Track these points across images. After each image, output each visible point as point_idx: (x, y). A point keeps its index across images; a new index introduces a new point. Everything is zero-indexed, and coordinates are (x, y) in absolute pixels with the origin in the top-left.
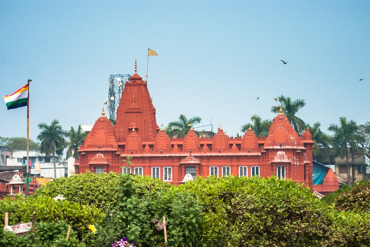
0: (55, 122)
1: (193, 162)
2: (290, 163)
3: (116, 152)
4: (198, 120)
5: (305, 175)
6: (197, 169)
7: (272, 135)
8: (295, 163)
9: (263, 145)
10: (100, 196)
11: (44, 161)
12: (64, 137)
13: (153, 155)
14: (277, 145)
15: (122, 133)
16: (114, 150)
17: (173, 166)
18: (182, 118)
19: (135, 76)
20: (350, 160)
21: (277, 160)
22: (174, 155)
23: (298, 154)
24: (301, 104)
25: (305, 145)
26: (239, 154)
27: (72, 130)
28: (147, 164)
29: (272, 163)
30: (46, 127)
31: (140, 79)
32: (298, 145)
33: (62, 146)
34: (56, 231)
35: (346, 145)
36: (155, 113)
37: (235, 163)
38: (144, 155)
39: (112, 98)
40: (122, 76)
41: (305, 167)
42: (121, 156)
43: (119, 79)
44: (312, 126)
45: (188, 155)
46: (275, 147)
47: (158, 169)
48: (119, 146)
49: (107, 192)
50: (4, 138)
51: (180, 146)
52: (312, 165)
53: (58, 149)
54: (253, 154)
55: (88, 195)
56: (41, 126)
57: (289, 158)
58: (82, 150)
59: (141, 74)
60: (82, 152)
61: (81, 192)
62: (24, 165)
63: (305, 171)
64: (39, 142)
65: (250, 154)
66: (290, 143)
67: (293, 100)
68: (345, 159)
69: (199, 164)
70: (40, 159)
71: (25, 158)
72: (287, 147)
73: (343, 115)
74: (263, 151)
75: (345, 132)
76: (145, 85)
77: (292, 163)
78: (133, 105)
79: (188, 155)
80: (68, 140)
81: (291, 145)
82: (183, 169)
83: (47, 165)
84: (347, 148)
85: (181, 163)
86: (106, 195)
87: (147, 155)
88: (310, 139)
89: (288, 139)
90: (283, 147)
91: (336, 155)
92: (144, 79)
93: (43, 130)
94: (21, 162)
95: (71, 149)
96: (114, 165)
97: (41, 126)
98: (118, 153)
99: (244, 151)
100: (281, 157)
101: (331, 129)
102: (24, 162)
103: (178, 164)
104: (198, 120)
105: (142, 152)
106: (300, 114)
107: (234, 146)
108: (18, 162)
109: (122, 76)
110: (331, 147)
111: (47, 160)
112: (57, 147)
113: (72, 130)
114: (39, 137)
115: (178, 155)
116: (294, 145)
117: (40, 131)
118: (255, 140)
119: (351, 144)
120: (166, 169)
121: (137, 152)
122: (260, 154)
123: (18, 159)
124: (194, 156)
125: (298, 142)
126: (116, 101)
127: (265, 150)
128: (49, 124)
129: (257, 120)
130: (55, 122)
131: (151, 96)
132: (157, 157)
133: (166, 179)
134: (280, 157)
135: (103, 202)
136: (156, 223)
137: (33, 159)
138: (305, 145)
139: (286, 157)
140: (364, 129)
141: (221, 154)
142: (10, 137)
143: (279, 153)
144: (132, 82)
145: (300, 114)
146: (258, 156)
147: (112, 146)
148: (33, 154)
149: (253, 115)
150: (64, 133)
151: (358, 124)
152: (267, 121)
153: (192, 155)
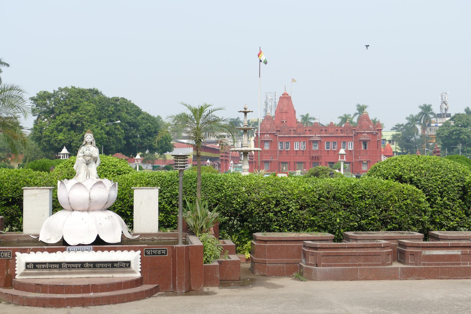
28: (292, 141)
31: (288, 95)
32: (374, 130)
38: (291, 135)
59: (288, 92)
76: (290, 98)
81: (371, 130)
92: (289, 95)
121: (287, 134)
125: (374, 128)
131: (293, 104)
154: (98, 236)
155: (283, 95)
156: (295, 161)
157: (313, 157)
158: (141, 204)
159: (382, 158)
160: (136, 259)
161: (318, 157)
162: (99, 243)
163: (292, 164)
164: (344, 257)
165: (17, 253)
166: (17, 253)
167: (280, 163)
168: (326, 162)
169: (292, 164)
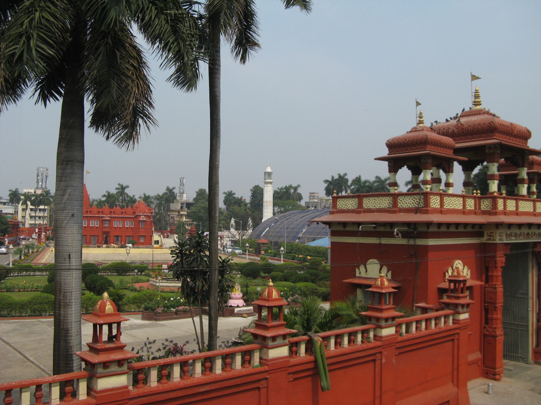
0: (17, 189)
24: (128, 187)
30: (12, 191)
44: (132, 196)
56: (10, 191)
67: (124, 185)
80: (22, 197)
83: (5, 206)
93: (11, 192)
97: (10, 191)
100: (143, 218)
106: (127, 191)
109: (43, 168)
117: (9, 193)
128: (14, 190)
129: (109, 193)
130: (17, 189)
134: (142, 218)
145: (127, 191)
169: (88, 237)
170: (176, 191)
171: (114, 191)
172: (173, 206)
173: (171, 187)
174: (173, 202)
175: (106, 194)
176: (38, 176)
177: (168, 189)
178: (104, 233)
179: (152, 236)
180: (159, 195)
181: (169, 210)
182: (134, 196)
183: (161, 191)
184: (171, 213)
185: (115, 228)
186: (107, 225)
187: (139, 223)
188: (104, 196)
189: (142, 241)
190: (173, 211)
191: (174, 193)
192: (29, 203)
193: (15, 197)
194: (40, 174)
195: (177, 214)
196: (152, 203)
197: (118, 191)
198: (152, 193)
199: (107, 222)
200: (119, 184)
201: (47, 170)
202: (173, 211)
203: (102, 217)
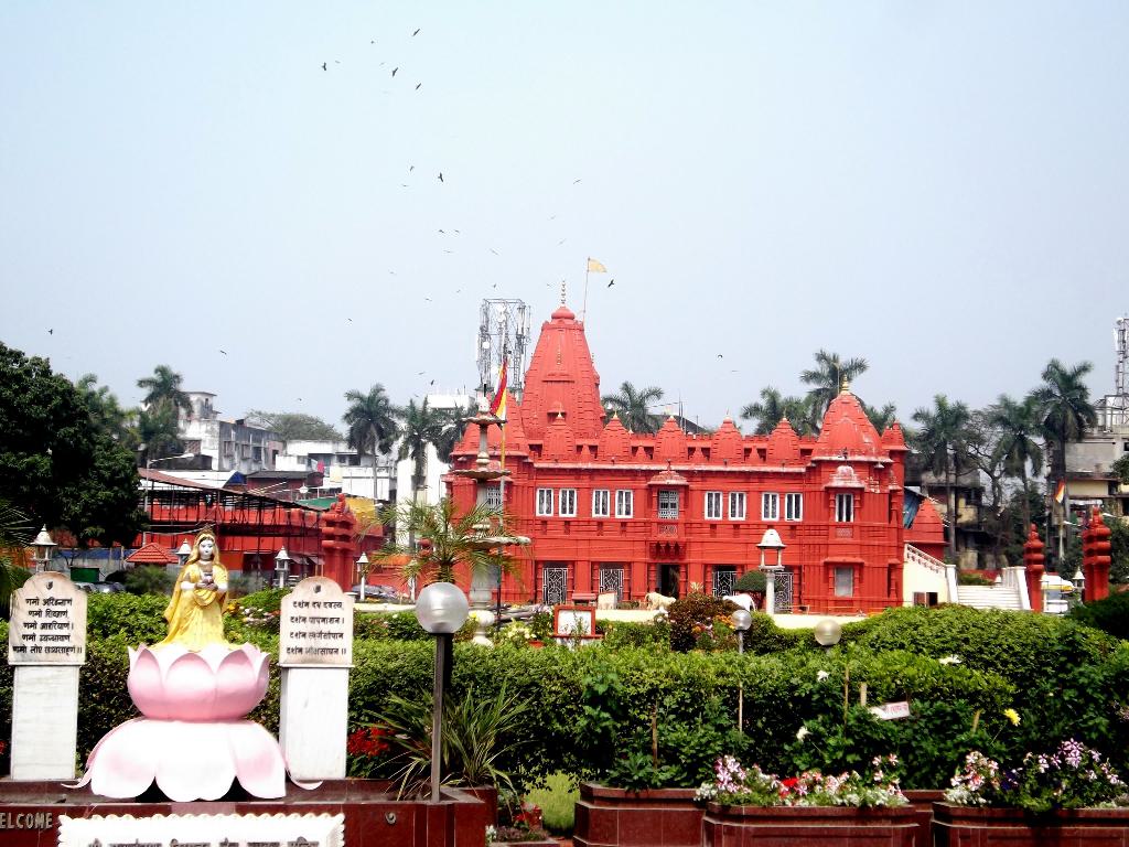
0: (378, 390)
1: (673, 482)
2: (861, 489)
3: (526, 457)
4: (657, 393)
5: (890, 512)
6: (682, 495)
7: (828, 433)
8: (873, 490)
9: (809, 452)
10: (1005, 656)
11: (347, 463)
12: (395, 420)
13: (596, 466)
14: (837, 453)
15: (535, 422)
16: (520, 453)
17: (634, 490)
18: (627, 388)
19: (561, 312)
20: (952, 478)
21: (837, 482)
22: (636, 467)
23: (878, 472)
25: (892, 454)
26: (763, 469)
27: (412, 406)
29: (828, 489)
31: (572, 318)
32: (879, 454)
33: (392, 437)
34: (948, 718)
35: (945, 449)
36: (597, 385)
37: (755, 486)
39: (486, 345)
40: (505, 303)
41: (890, 498)
42: (536, 465)
43: (500, 308)
44: (880, 410)
45: (664, 467)
46: (835, 458)
47: (605, 493)
48: (531, 446)
49: (1018, 649)
50: (266, 415)
51: (649, 450)
52: (902, 493)
53: (384, 441)
54: (791, 470)
55: (981, 651)
56: (350, 396)
57: (861, 478)
58: (460, 453)
59: (573, 307)
60: (460, 456)
61: (966, 647)
62: (309, 469)
63: (890, 504)
64: (344, 429)
65: (785, 470)
66: (863, 450)
67: (844, 360)
68: (943, 478)
69: (686, 487)
70: (341, 458)
71: (312, 456)
72: (858, 458)
73: (941, 392)
74: (809, 465)
75: (944, 424)
76: (582, 330)
77: (867, 489)
78: (558, 369)
79: (664, 467)
80: (402, 424)
82: (655, 495)
83: (355, 471)
84: (947, 454)
85: (651, 482)
86: (1015, 654)
87: (585, 466)
88: (900, 443)
89: (860, 443)
90: (849, 459)
91: (926, 469)
93: (354, 403)
94: (303, 463)
95: (406, 442)
96: (521, 483)
97: (350, 396)
98: (530, 460)
99: (772, 464)
100: (846, 476)
101: (917, 416)
102: (310, 464)
103: (644, 485)
104: (657, 393)
105: (575, 460)
107: (754, 454)
108: (298, 462)
109: (505, 303)
110: (915, 451)
111: (355, 461)
112: (381, 437)
113: (412, 406)
114: (347, 416)
115: (644, 467)
116: (872, 455)
117: (347, 406)
118: (794, 443)
119: (955, 449)
120: (621, 493)
121: (566, 460)
122: (803, 470)
123: (299, 457)
124: (677, 471)
125: (879, 447)
126: (494, 351)
127: (813, 462)
128: (366, 393)
129: (773, 398)
130: (378, 390)
132: (604, 470)
133: (620, 513)
134: (844, 478)
135: (1011, 666)
136: (1118, 708)
137: (328, 456)
138: (892, 454)
139: (854, 475)
140: (981, 419)
141: (728, 469)
142: (278, 412)
143: (841, 468)
144: (556, 322)
145: (855, 387)
146: (800, 474)
147: (518, 446)
148: (326, 448)
149: (765, 387)
150: (394, 411)
151: (971, 408)
152: (791, 398)
153: (673, 467)
154: (236, 782)
155: (553, 318)
156: (593, 559)
157: (658, 545)
158: (306, 705)
159: (906, 551)
160: (333, 835)
161: (677, 546)
162: (238, 798)
163: (583, 570)
164: (805, 839)
165: (63, 818)
166: (63, 818)
167: (540, 566)
168: (706, 565)
169: (583, 570)
170: (1098, 387)
171: (796, 390)
172: (1082, 457)
173: (1068, 366)
174: (1080, 437)
175: (763, 403)
176: (485, 333)
177: (1053, 371)
178: (658, 549)
179: (894, 572)
180: (1007, 404)
181: (1060, 475)
182: (889, 410)
183: (1023, 384)
184: (1076, 490)
185: (713, 526)
186: (671, 514)
187: (828, 502)
188: (752, 411)
189: (843, 592)
190: (1084, 479)
191: (1082, 389)
192: (431, 450)
193: (371, 425)
194: (493, 330)
195: (1103, 492)
196: (978, 440)
197: (814, 386)
198: (978, 397)
199: (675, 499)
200: (822, 357)
201: (522, 309)
202: (1084, 479)
203: (649, 474)
